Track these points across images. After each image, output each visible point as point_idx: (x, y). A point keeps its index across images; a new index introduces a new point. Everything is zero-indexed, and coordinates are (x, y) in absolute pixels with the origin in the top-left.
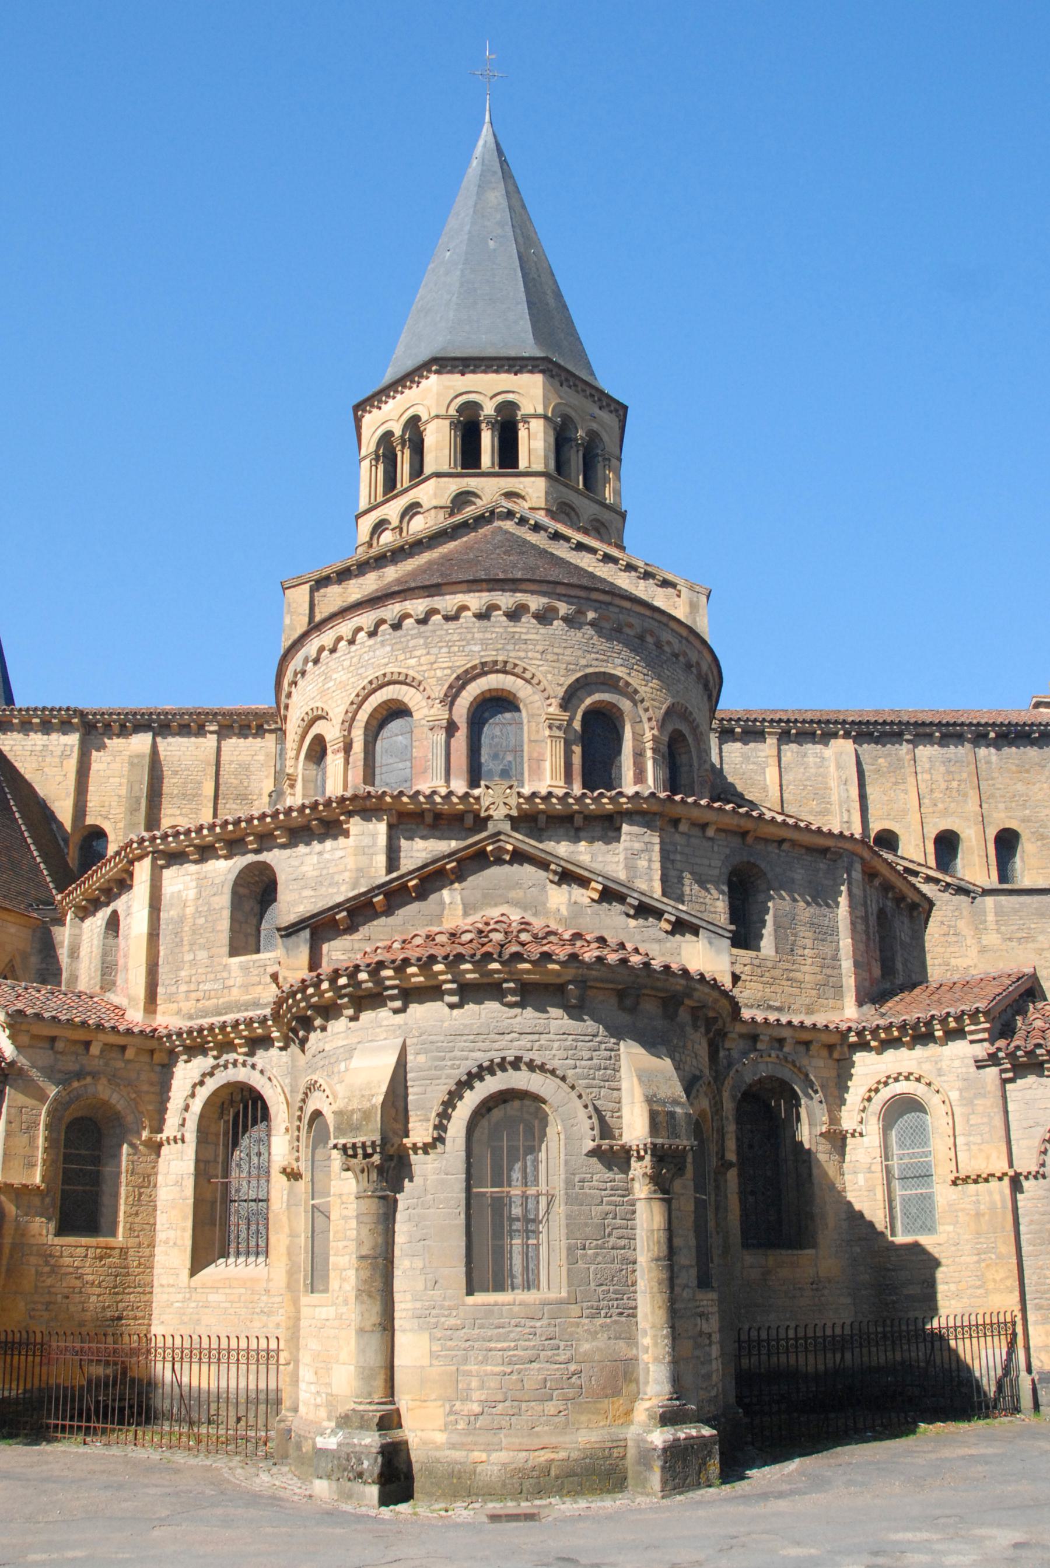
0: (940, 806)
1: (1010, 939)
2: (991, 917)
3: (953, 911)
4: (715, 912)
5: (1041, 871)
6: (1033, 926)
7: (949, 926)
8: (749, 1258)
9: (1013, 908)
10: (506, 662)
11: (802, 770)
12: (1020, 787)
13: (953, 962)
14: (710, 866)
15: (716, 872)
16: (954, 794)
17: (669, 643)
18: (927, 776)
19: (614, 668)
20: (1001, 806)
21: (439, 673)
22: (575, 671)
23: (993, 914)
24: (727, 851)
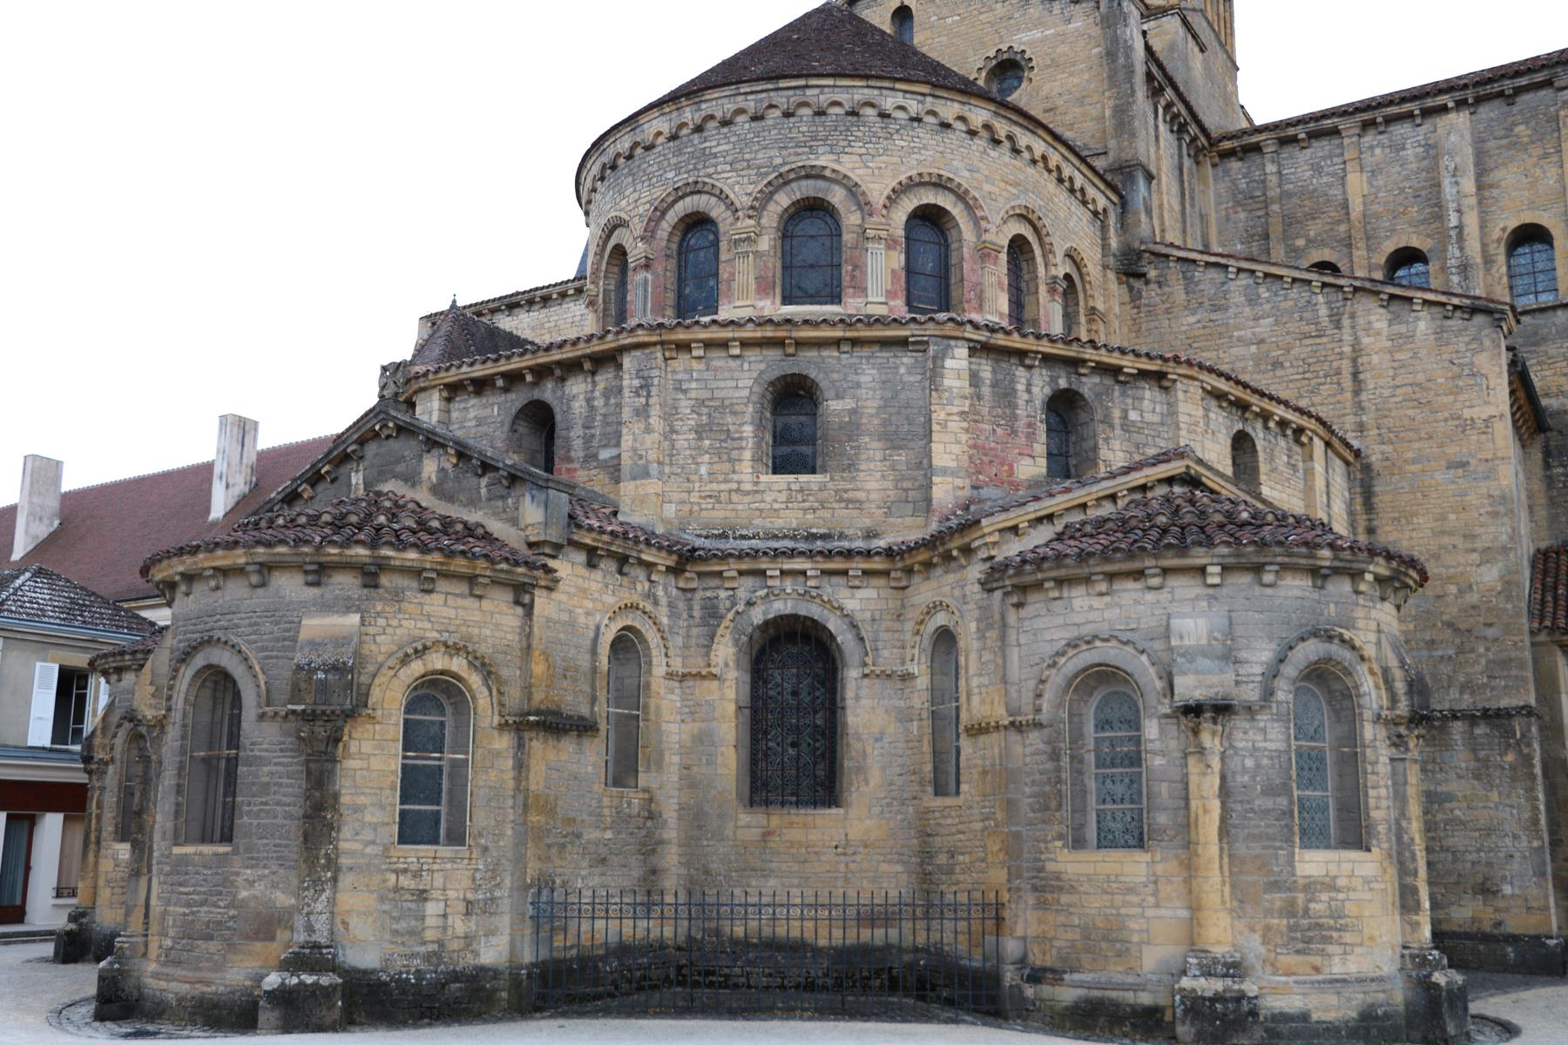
4: (741, 439)
7: (1460, 365)
8: (745, 818)
10: (696, 183)
11: (1398, 169)
13: (1467, 413)
14: (737, 387)
15: (746, 393)
17: (902, 108)
19: (817, 159)
21: (641, 210)
22: (767, 174)
24: (762, 366)
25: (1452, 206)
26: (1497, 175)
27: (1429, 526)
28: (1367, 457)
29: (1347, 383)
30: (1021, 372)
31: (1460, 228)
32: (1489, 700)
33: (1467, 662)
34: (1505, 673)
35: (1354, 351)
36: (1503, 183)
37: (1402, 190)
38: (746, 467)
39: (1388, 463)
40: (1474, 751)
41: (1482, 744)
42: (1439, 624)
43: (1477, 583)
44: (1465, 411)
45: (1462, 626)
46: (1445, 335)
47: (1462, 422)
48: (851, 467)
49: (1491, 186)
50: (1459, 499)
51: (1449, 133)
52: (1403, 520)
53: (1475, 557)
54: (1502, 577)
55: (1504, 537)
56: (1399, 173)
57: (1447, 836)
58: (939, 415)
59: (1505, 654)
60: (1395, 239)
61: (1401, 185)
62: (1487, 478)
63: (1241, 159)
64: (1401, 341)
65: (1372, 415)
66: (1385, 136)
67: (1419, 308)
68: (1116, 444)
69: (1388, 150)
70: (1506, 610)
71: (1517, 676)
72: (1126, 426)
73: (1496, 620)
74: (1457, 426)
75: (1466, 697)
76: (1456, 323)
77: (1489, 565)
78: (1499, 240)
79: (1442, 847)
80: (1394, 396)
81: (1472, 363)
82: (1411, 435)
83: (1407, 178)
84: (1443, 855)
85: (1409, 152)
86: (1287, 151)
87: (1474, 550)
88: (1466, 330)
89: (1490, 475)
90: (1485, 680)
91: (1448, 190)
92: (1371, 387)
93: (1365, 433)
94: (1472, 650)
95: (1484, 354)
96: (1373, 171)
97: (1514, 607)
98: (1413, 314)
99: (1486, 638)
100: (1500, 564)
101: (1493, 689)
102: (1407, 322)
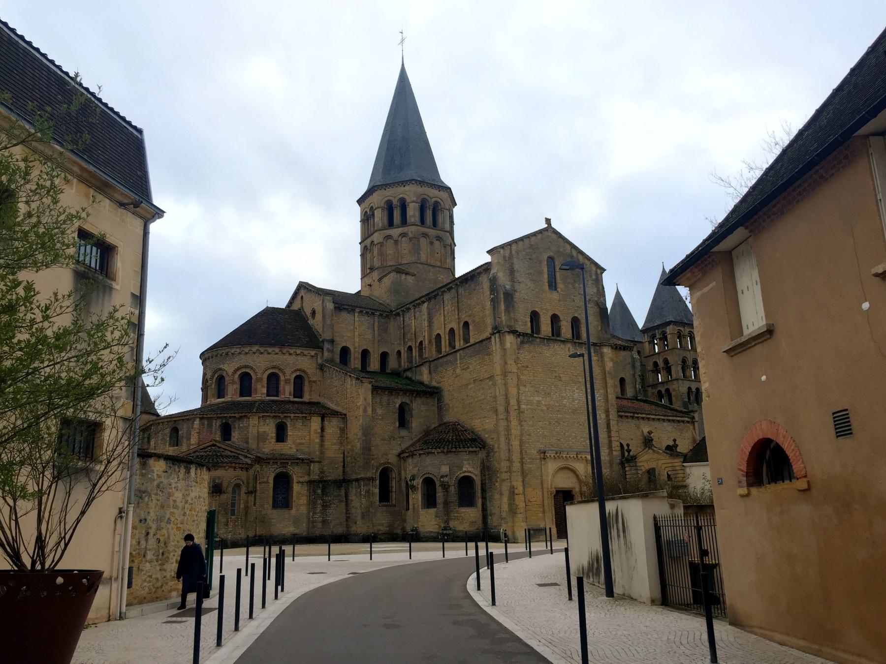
30: (214, 421)
38: (167, 446)
48: (182, 445)
58: (193, 433)
68: (236, 432)
72: (239, 428)
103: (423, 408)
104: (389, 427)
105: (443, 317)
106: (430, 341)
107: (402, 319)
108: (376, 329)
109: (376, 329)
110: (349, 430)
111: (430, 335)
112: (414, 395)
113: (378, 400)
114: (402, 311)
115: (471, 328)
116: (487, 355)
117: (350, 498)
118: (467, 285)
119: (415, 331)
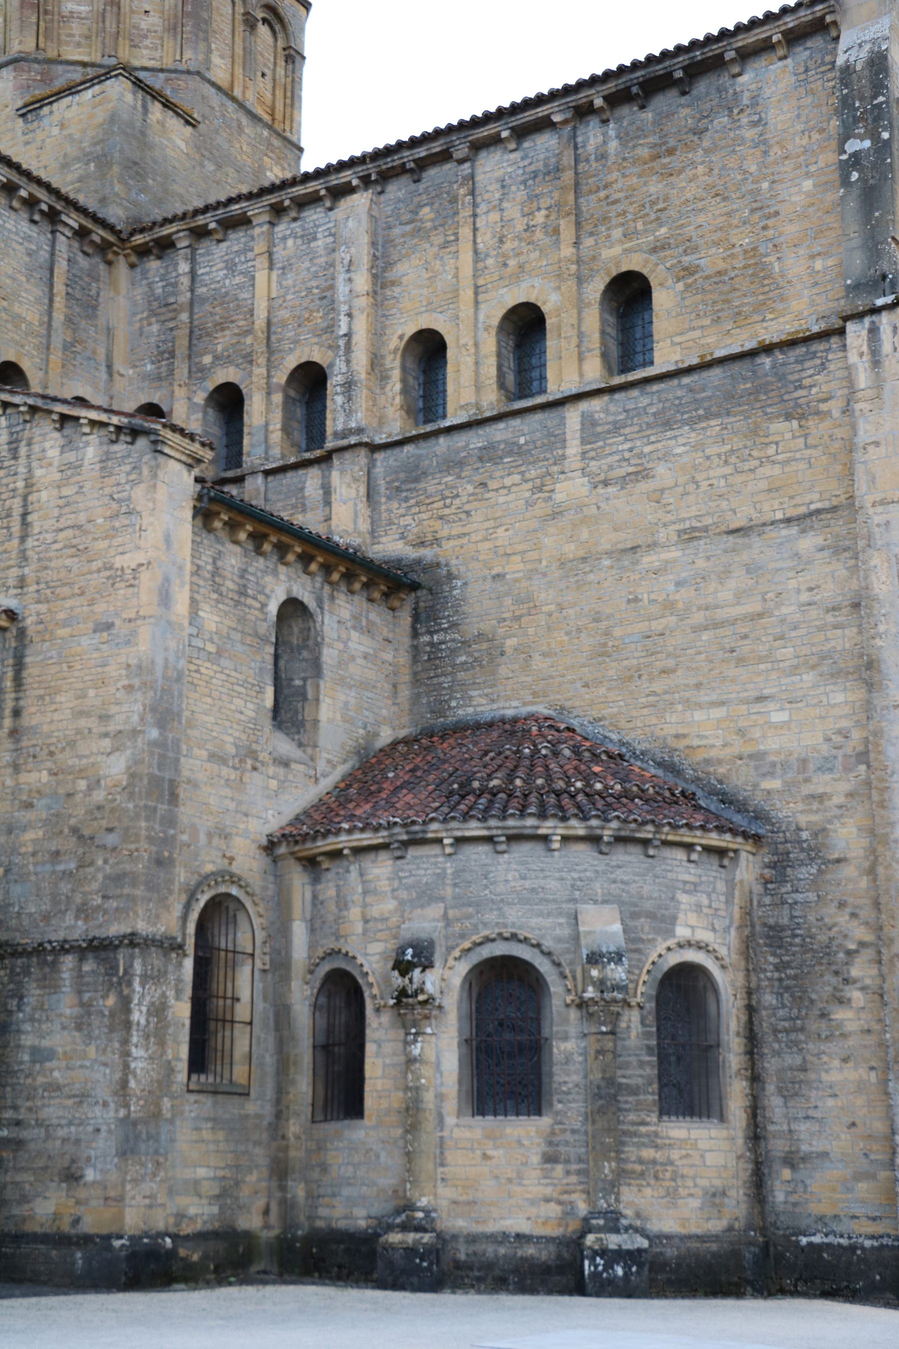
0: (512, 263)
1: (606, 483)
2: (573, 449)
3: (128, 474)
5: (678, 339)
6: (647, 449)
7: (119, 501)
9: (615, 423)
12: (655, 187)
13: (118, 562)
16: (539, 235)
18: (494, 216)
20: (617, 233)
23: (577, 442)
25: (344, 308)
26: (400, 269)
27: (70, 705)
28: (24, 619)
29: (16, 528)
31: (348, 335)
32: (100, 926)
33: (85, 878)
34: (118, 892)
35: (26, 487)
36: (404, 280)
37: (309, 290)
39: (41, 627)
40: (80, 992)
41: (87, 984)
42: (66, 831)
43: (106, 777)
44: (118, 558)
45: (86, 832)
46: (110, 463)
47: (112, 572)
49: (393, 283)
50: (100, 669)
51: (348, 218)
52: (47, 698)
53: (107, 743)
54: (129, 768)
55: (135, 718)
56: (308, 269)
57: (44, 1106)
59: (122, 866)
60: (298, 352)
61: (309, 284)
62: (128, 643)
63: (159, 258)
64: (69, 473)
65: (33, 567)
66: (299, 223)
67: (87, 430)
69: (299, 242)
70: (126, 810)
71: (128, 895)
73: (116, 824)
74: (108, 578)
75: (80, 923)
76: (120, 448)
77: (117, 754)
78: (396, 350)
79: (37, 1120)
80: (55, 542)
81: (129, 499)
82: (65, 591)
83: (316, 276)
84: (36, 1131)
85: (320, 243)
86: (204, 246)
87: (106, 735)
88: (129, 456)
89: (130, 640)
90: (99, 901)
91: (342, 289)
92: (36, 531)
93: (25, 590)
94: (92, 864)
95: (142, 485)
96: (283, 268)
97: (135, 807)
98: (84, 438)
99: (104, 847)
100: (129, 752)
101: (105, 912)
102: (77, 449)
103: (358, 643)
104: (238, 702)
105: (467, 257)
106: (375, 361)
107: (184, 267)
108: (59, 287)
109: (59, 287)
110: (32, 691)
111: (378, 334)
112: (335, 576)
113: (206, 559)
114: (191, 230)
115: (662, 299)
116: (788, 417)
117: (28, 1040)
118: (648, 116)
119: (269, 324)
